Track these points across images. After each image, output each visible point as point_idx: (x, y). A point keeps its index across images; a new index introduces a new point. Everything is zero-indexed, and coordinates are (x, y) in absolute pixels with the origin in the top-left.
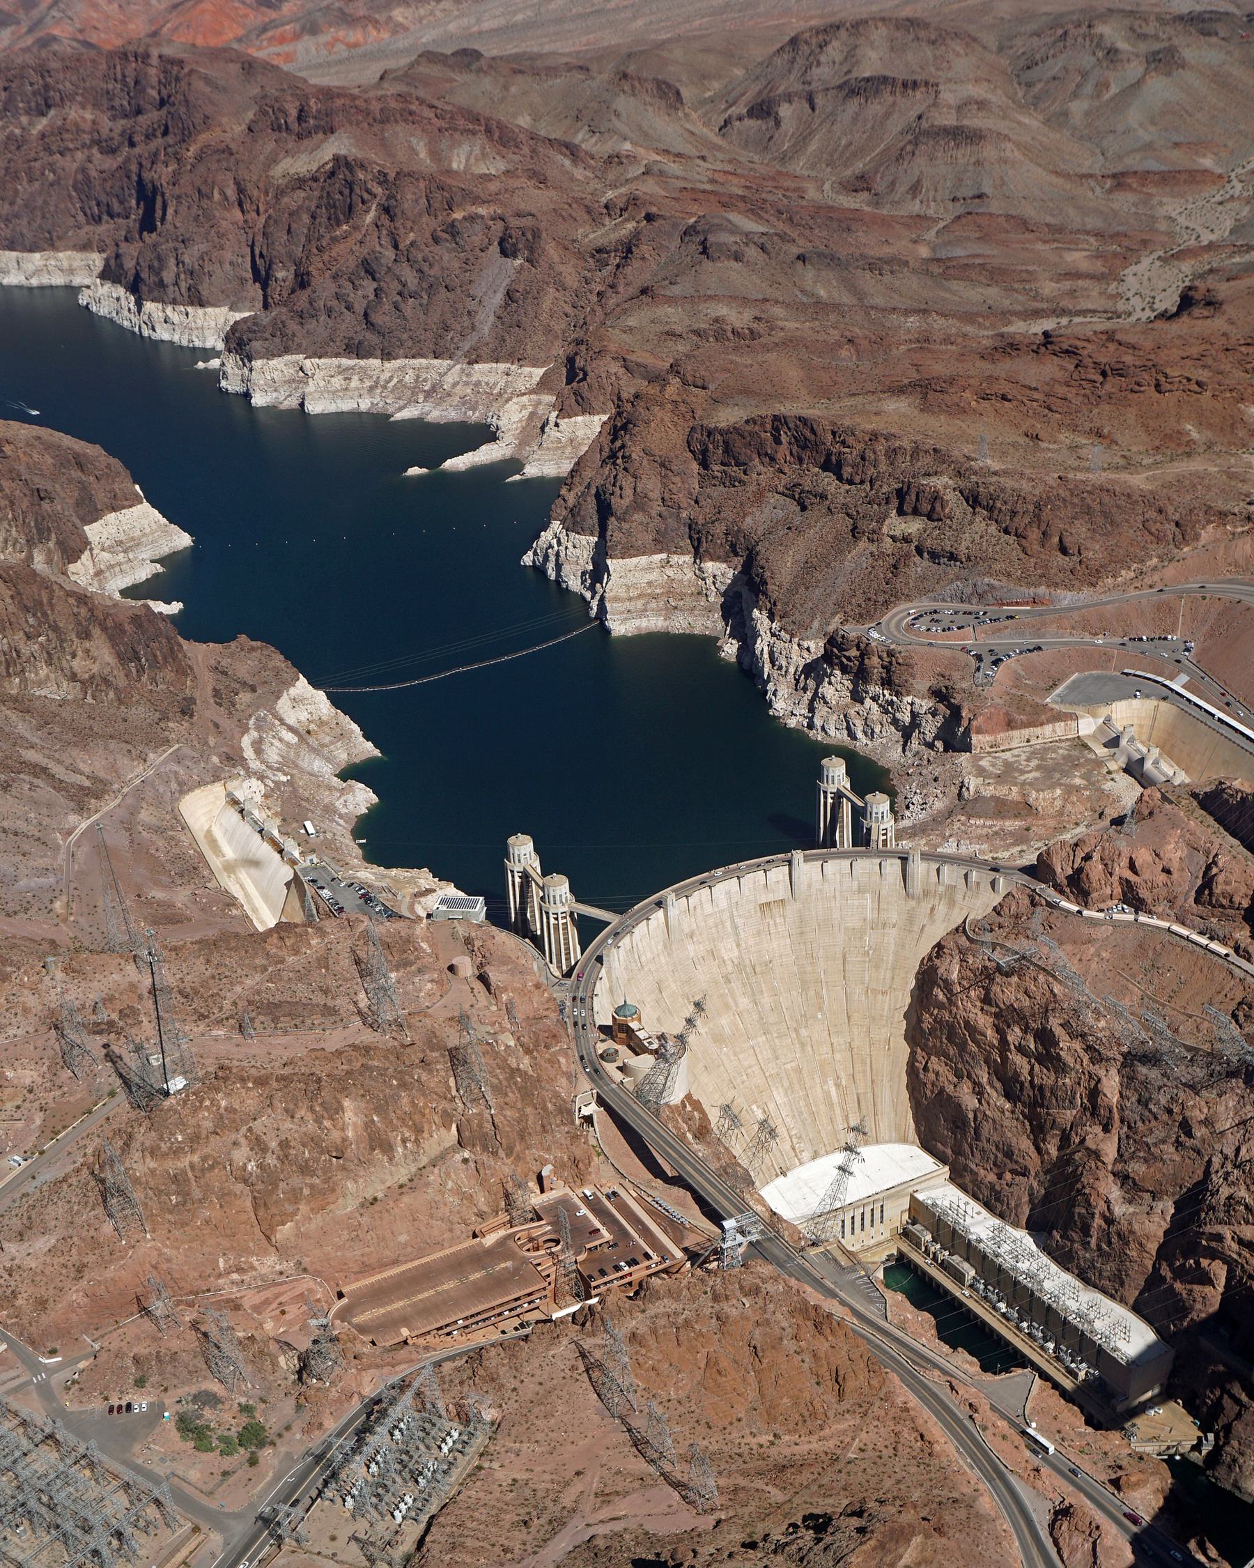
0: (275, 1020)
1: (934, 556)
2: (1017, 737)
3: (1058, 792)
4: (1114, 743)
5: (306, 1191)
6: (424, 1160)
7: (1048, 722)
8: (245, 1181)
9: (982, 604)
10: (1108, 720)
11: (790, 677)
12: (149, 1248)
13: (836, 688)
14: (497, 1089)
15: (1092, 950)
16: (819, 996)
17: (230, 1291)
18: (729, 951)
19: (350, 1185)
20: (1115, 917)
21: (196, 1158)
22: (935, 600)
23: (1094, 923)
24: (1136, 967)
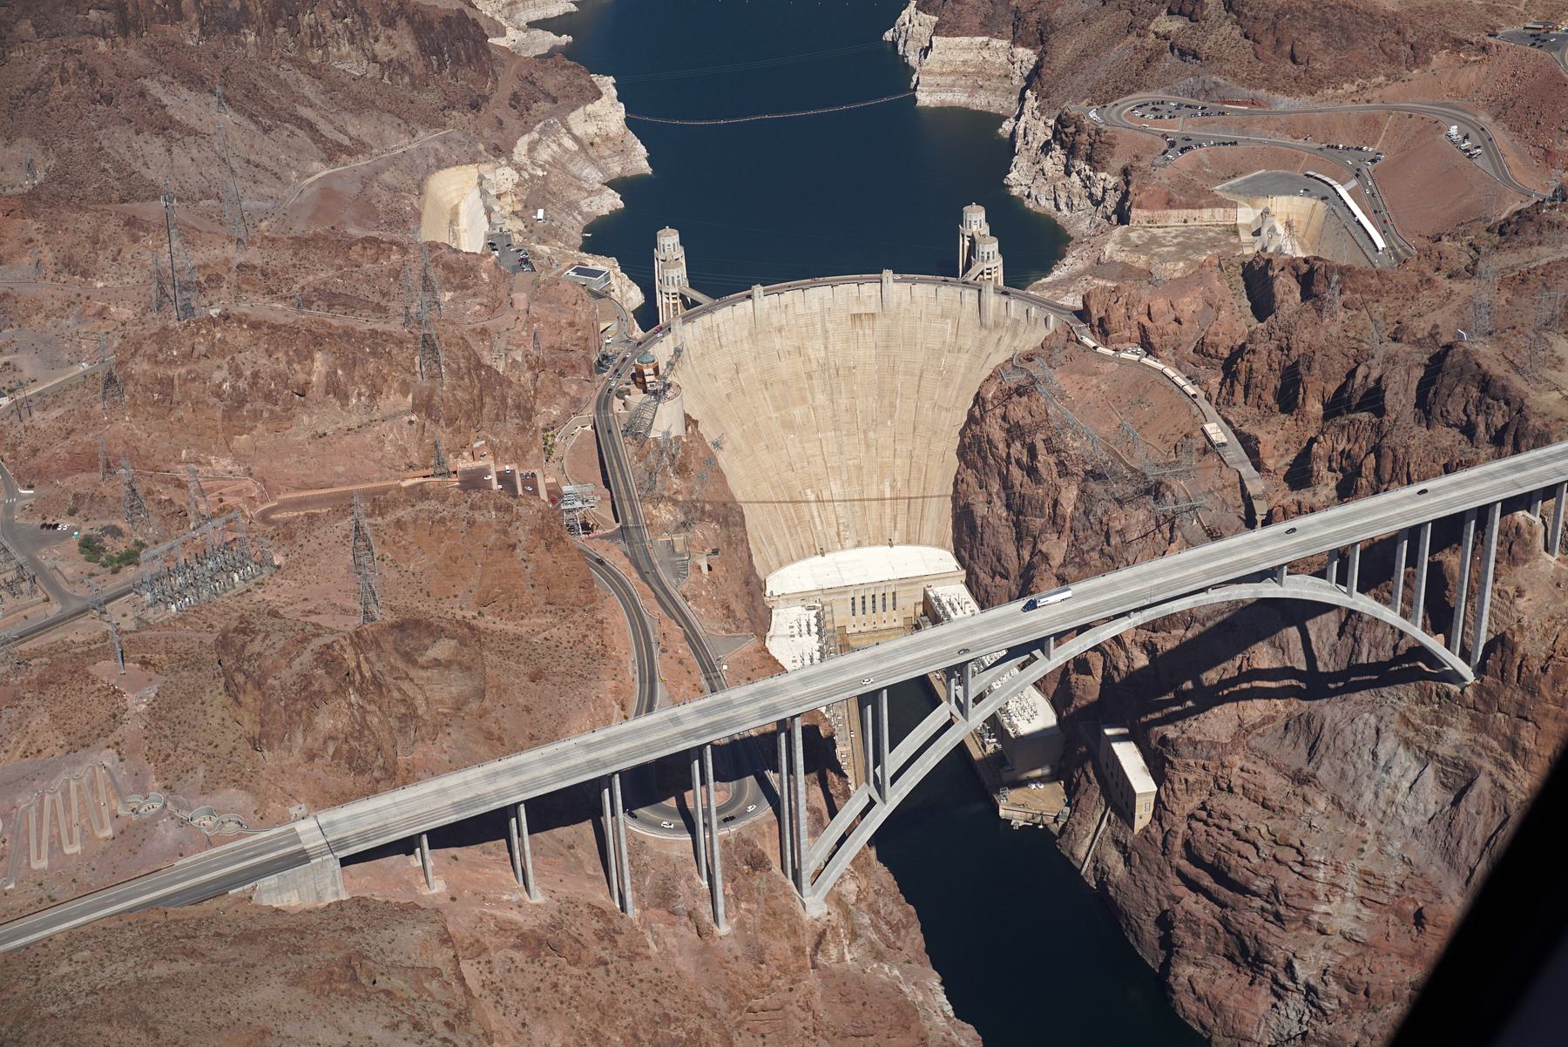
0: (330, 306)
1: (1183, 54)
2: (1175, 217)
3: (1181, 264)
4: (1257, 233)
5: (266, 415)
6: (378, 416)
7: (1209, 206)
8: (219, 396)
9: (1207, 101)
10: (1266, 212)
11: (1032, 152)
12: (123, 426)
13: (1053, 163)
14: (457, 374)
15: (1095, 381)
16: (892, 405)
17: (182, 473)
18: (815, 350)
19: (306, 418)
20: (1123, 355)
21: (183, 371)
22: (1169, 93)
23: (1104, 358)
24: (1124, 401)
